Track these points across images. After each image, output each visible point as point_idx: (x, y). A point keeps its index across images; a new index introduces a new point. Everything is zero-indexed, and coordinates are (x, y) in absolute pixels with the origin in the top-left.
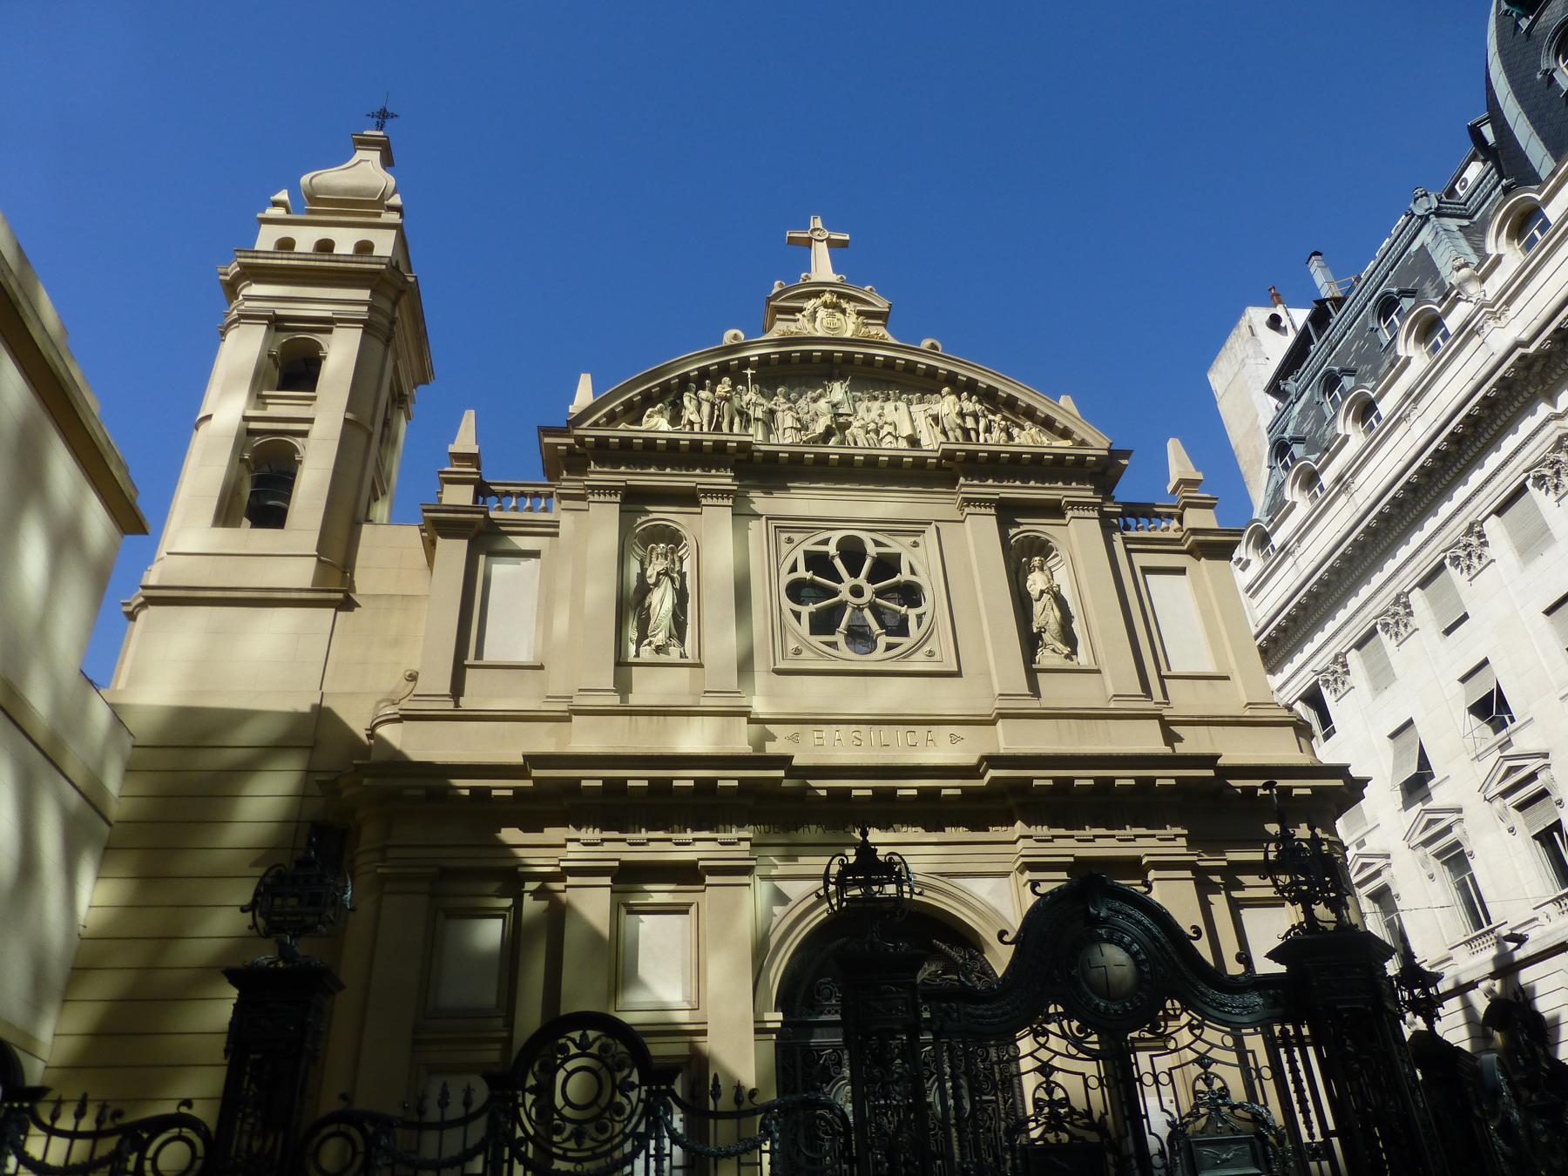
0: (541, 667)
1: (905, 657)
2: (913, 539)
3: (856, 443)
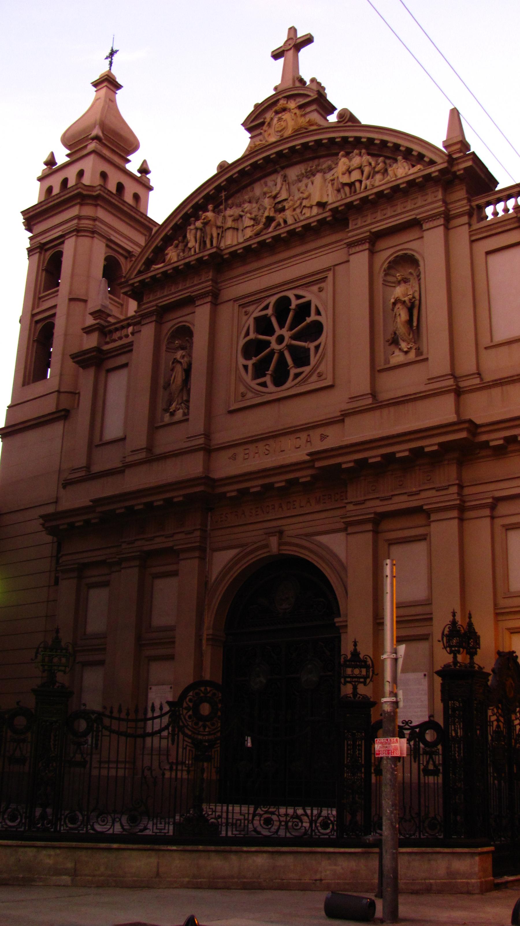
0: (123, 439)
1: (304, 382)
3: (285, 222)
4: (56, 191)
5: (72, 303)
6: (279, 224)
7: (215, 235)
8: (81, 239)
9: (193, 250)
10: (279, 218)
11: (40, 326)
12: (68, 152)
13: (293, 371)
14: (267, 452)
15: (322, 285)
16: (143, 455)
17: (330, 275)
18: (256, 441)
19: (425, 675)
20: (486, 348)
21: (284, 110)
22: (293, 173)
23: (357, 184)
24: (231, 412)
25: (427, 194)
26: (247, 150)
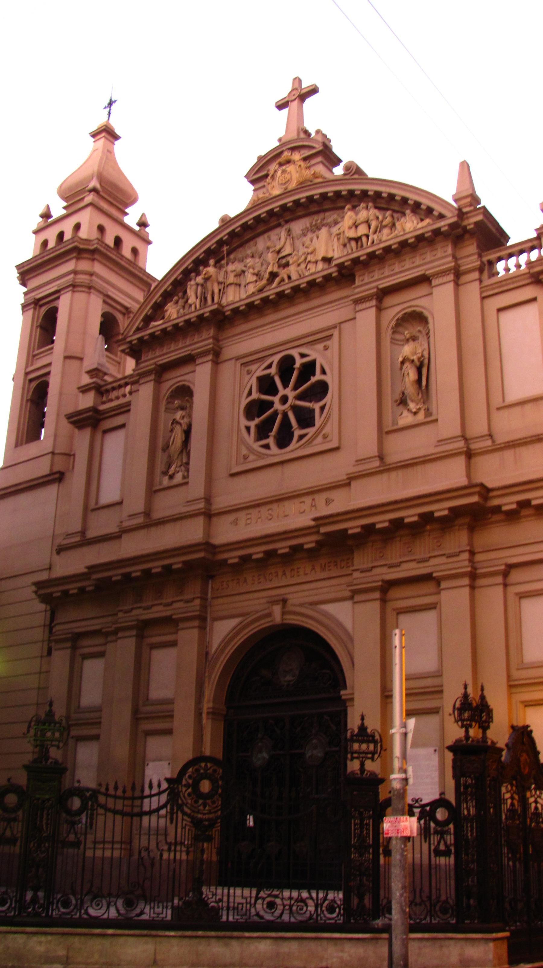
0: (120, 503)
2: (325, 344)
3: (289, 277)
4: (52, 244)
5: (68, 361)
6: (283, 280)
7: (216, 291)
8: (77, 295)
9: (193, 307)
10: (283, 273)
11: (34, 384)
12: (65, 204)
13: (297, 433)
14: (270, 517)
15: (328, 343)
16: (140, 520)
17: (336, 333)
18: (258, 505)
19: (435, 750)
20: (498, 409)
21: (288, 162)
22: (297, 227)
23: (364, 239)
24: (233, 475)
25: (436, 249)
26: (250, 203)
